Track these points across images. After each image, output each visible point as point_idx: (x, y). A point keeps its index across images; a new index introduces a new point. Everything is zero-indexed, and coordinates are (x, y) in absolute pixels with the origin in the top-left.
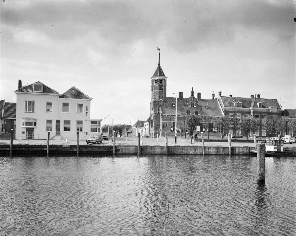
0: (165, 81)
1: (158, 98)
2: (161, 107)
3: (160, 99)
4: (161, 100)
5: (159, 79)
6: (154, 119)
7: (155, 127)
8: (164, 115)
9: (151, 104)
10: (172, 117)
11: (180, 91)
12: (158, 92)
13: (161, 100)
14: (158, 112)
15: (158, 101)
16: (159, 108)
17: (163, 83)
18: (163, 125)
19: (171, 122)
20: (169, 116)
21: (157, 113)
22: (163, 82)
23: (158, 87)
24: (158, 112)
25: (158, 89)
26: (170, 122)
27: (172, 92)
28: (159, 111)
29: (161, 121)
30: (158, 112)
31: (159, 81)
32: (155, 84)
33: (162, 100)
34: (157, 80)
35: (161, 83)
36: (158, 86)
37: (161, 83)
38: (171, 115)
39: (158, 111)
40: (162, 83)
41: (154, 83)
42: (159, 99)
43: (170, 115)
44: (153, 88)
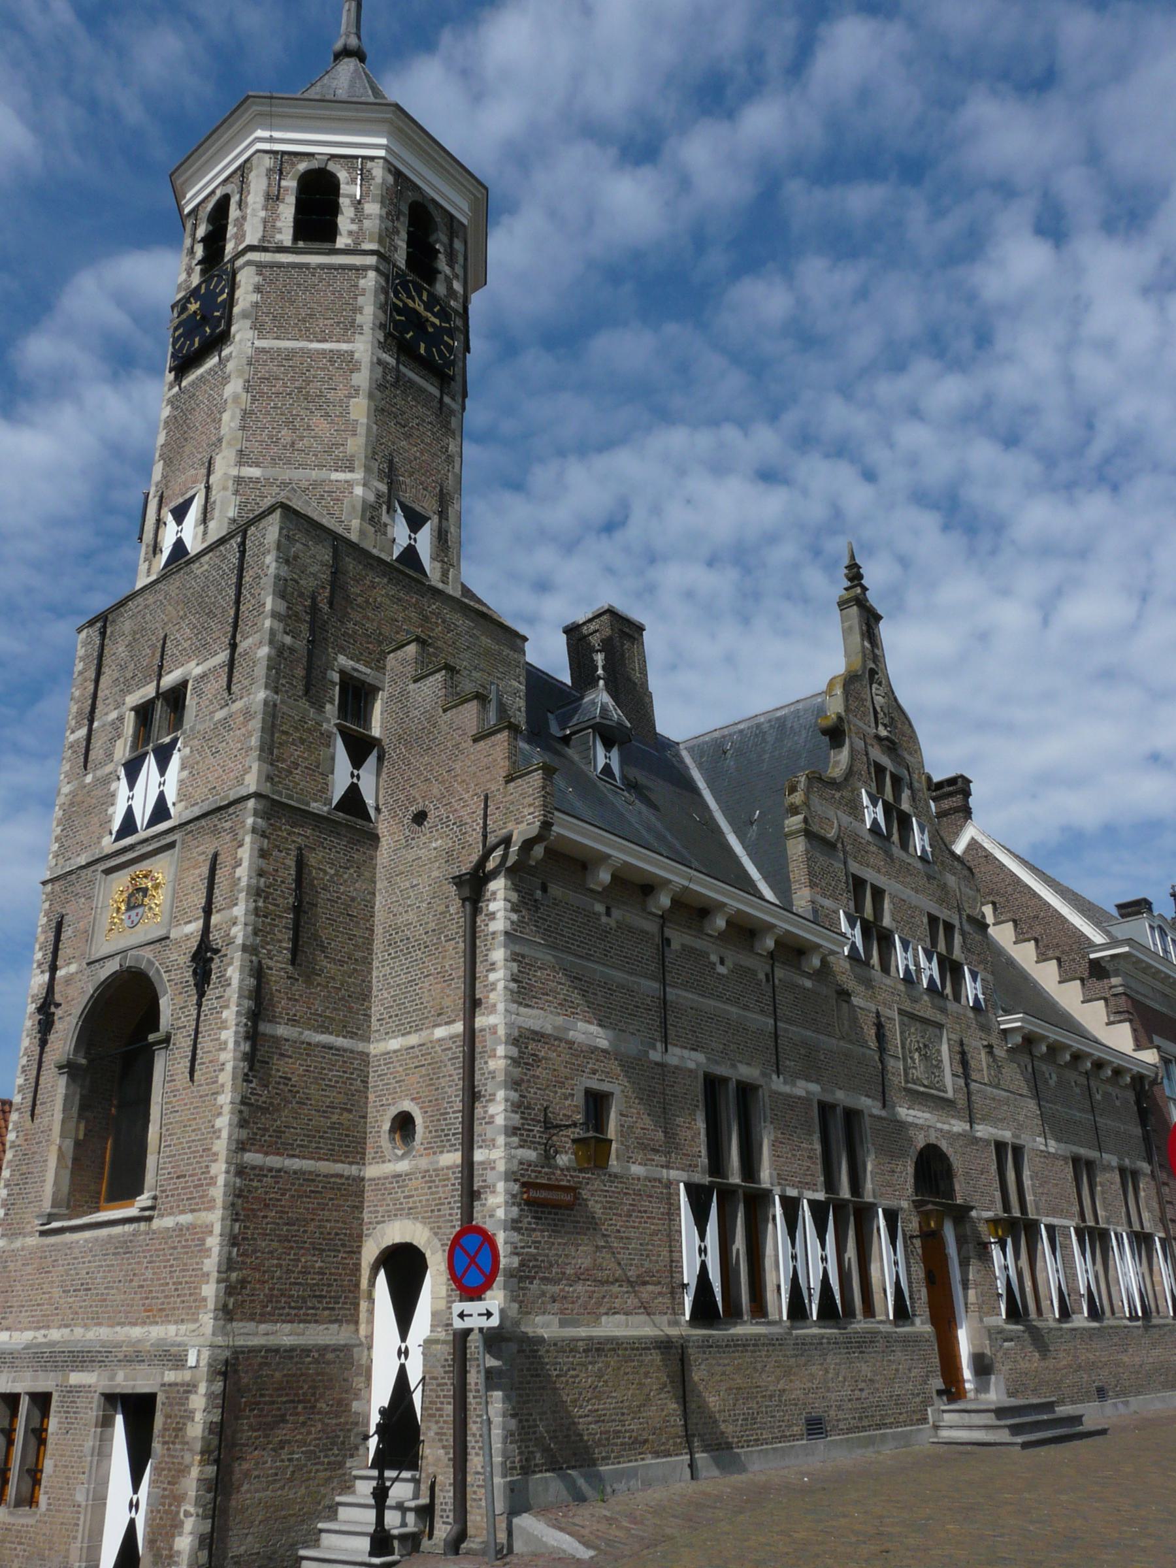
1: (357, 486)
3: (400, 532)
4: (410, 553)
5: (398, 174)
6: (235, 920)
10: (679, 938)
12: (362, 378)
13: (410, 553)
14: (338, 792)
15: (353, 528)
18: (534, 1123)
21: (325, 788)
24: (353, 793)
25: (368, 313)
26: (655, 1056)
28: (372, 760)
32: (286, 237)
34: (366, 177)
36: (361, 270)
41: (287, 212)
42: (372, 515)
44: (245, 297)
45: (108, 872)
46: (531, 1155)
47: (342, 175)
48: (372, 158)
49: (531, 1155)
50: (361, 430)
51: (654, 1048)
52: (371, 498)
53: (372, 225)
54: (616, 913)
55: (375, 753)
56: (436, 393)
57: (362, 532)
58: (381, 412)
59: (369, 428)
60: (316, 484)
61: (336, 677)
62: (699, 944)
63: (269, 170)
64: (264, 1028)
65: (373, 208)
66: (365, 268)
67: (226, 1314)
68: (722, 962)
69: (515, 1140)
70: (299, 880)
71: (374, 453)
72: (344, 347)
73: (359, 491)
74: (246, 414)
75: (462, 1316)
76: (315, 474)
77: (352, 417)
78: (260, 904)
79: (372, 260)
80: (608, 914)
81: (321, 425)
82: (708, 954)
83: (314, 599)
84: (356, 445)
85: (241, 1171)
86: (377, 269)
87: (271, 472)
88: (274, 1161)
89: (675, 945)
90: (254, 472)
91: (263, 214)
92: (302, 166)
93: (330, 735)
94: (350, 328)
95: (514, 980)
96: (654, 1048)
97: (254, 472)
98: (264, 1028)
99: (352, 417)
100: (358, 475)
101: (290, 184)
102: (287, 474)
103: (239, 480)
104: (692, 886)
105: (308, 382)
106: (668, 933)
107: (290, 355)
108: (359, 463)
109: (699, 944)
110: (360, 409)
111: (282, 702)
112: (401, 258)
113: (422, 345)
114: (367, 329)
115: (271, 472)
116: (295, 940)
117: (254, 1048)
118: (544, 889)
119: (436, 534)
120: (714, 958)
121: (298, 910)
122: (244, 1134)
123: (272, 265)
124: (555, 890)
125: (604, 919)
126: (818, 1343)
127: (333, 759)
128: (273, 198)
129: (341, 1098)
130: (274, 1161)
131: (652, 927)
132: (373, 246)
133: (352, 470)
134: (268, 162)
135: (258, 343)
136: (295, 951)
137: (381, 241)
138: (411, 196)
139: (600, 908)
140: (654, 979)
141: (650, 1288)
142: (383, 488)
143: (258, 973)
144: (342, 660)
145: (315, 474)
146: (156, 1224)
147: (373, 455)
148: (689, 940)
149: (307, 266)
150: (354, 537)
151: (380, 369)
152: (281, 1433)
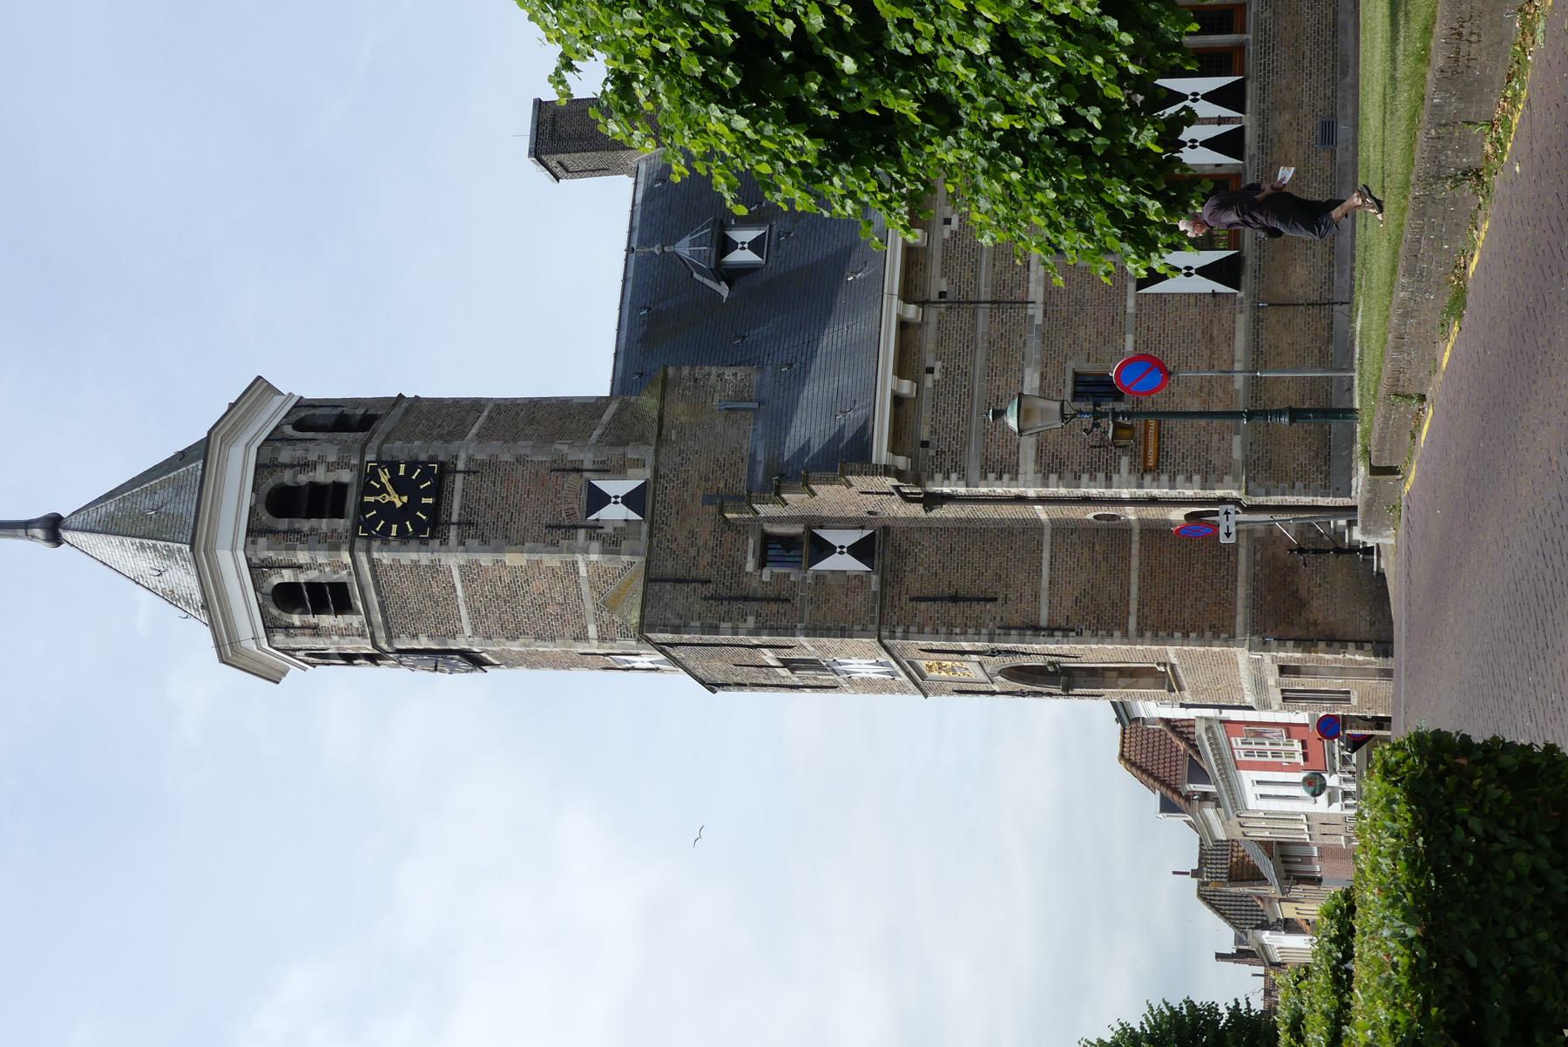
0: (312, 419)
1: (589, 561)
2: (744, 501)
3: (614, 513)
4: (630, 500)
7: (1160, 626)
8: (895, 448)
9: (723, 685)
10: (938, 283)
11: (525, 143)
12: (486, 559)
13: (630, 500)
16: (775, 548)
17: (329, 464)
19: (1036, 292)
20: (931, 332)
21: (858, 577)
22: (306, 466)
23: (385, 558)
24: (857, 550)
26: (1037, 312)
27: (527, 296)
28: (829, 535)
29: (1031, 496)
30: (857, 550)
31: (295, 538)
32: (355, 621)
33: (619, 472)
35: (325, 501)
36: (373, 564)
37: (325, 501)
38: (907, 296)
39: (826, 549)
40: (321, 476)
41: (326, 620)
43: (893, 308)
45: (923, 677)
46: (1125, 462)
47: (276, 580)
48: (248, 560)
49: (1125, 462)
50: (536, 557)
51: (1032, 317)
52: (595, 545)
53: (322, 557)
54: (929, 363)
55: (818, 532)
56: (459, 478)
57: (633, 553)
58: (511, 540)
59: (531, 551)
60: (593, 587)
61: (766, 574)
62: (937, 255)
63: (287, 635)
64: (1044, 622)
65: (302, 557)
66: (371, 561)
67: (1231, 639)
68: (948, 221)
69: (1115, 477)
70: (934, 599)
71: (552, 544)
72: (456, 573)
73: (594, 557)
74: (539, 637)
75: (1228, 535)
76: (585, 588)
77: (524, 563)
78: (958, 630)
79: (362, 558)
80: (930, 370)
81: (538, 585)
82: (945, 241)
83: (706, 598)
84: (552, 560)
85: (1141, 633)
86: (368, 551)
87: (590, 617)
88: (1133, 606)
89: (944, 286)
90: (592, 631)
91: (335, 638)
92: (275, 612)
93: (819, 576)
94: (434, 568)
95: (1000, 478)
96: (1032, 317)
97: (592, 631)
98: (1044, 622)
99: (524, 563)
100: (579, 557)
101: (296, 619)
102: (589, 607)
103: (602, 639)
104: (896, 291)
105: (498, 597)
106: (934, 296)
107: (474, 612)
108: (568, 557)
109: (937, 255)
110: (515, 559)
111: (801, 621)
112: (342, 524)
113: (424, 501)
114: (436, 556)
115: (590, 617)
116: (979, 600)
117: (1059, 629)
118: (925, 444)
119: (602, 475)
120: (947, 234)
121: (955, 599)
122: (1117, 633)
123: (388, 630)
124: (925, 434)
125: (937, 375)
126: (1264, 118)
127: (833, 572)
128: (316, 631)
129: (1086, 552)
130: (1133, 606)
131: (933, 314)
132: (346, 557)
133: (575, 563)
134: (280, 638)
135: (468, 631)
136: (987, 600)
137: (338, 549)
138: (265, 517)
139: (929, 381)
140: (974, 315)
141: (1215, 333)
142: (582, 533)
143: (1007, 629)
144: (750, 567)
145: (585, 588)
146: (1174, 660)
147: (554, 546)
148: (936, 268)
149: (381, 604)
150: (639, 560)
151: (469, 542)
152: (1303, 593)
